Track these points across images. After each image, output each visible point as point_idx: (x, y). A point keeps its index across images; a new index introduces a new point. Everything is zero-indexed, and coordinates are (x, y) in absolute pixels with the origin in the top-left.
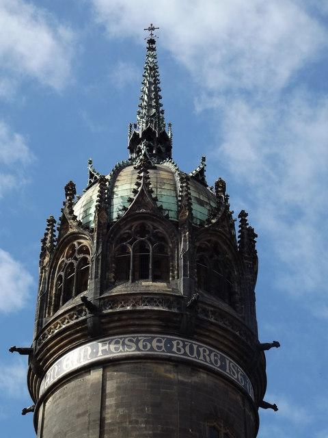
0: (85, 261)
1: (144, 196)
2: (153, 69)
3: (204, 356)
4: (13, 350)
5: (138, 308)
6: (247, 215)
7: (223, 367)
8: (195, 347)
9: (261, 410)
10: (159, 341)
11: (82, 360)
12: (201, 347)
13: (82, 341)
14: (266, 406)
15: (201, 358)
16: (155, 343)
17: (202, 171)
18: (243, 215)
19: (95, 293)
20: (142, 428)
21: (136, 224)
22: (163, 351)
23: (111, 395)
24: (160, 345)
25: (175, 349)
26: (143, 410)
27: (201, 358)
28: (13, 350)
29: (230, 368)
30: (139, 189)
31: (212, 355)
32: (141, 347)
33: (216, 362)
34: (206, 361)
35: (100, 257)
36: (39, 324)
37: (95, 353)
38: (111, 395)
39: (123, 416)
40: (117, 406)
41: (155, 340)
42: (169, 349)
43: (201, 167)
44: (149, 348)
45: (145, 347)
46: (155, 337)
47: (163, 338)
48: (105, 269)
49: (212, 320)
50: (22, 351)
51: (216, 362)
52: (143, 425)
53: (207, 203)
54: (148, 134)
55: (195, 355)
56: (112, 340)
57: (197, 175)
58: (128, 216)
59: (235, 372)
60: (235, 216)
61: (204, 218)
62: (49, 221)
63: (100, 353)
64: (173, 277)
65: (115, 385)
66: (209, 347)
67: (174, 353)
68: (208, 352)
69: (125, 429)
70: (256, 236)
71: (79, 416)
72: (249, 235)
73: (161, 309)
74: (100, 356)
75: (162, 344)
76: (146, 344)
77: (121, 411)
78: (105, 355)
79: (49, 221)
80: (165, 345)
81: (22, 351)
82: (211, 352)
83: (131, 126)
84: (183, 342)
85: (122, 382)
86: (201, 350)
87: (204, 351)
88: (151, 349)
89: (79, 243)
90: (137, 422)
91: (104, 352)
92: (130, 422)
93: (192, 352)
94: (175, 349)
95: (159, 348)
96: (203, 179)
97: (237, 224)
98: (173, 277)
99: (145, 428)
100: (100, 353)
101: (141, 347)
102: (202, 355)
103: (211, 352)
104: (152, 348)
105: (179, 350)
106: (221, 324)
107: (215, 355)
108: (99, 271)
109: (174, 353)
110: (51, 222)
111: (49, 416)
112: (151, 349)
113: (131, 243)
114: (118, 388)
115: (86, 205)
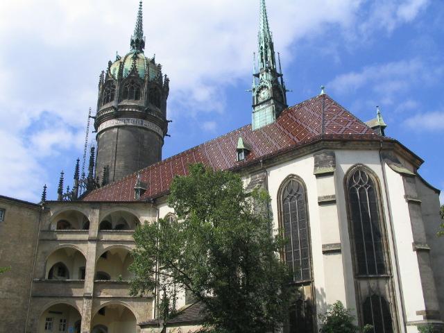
1: (134, 70)
2: (140, 13)
9: (166, 138)
14: (167, 135)
17: (153, 60)
18: (166, 76)
21: (131, 80)
36: (98, 109)
42: (142, 124)
48: (120, 94)
54: (137, 40)
58: (129, 77)
59: (160, 132)
72: (167, 80)
97: (164, 78)
110: (103, 72)
115: (115, 69)
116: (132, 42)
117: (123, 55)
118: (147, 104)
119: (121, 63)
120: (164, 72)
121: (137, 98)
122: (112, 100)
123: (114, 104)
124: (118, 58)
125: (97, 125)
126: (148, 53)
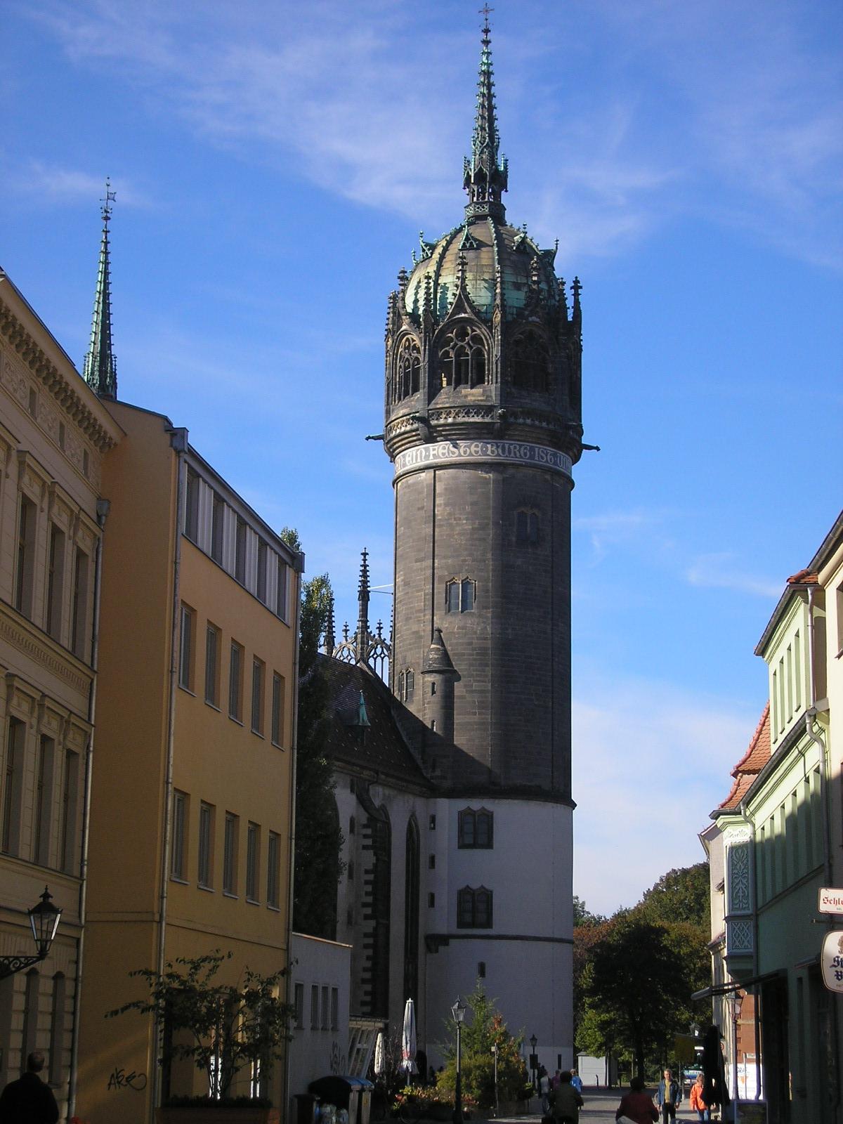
0: (417, 359)
2: (488, 74)
3: (515, 452)
4: (367, 439)
5: (460, 420)
7: (532, 457)
8: (507, 446)
10: (477, 446)
11: (419, 460)
12: (512, 444)
13: (417, 443)
15: (512, 455)
16: (473, 448)
19: (424, 405)
20: (463, 524)
22: (480, 455)
23: (441, 495)
25: (489, 452)
26: (464, 509)
27: (512, 455)
28: (367, 439)
29: (539, 453)
30: (458, 293)
31: (522, 449)
32: (462, 454)
33: (525, 454)
34: (517, 457)
35: (427, 366)
37: (427, 457)
38: (441, 495)
39: (450, 514)
40: (446, 505)
41: (473, 446)
43: (522, 235)
44: (468, 453)
45: (465, 452)
49: (521, 421)
51: (525, 454)
52: (465, 522)
53: (525, 284)
54: (480, 176)
55: (507, 453)
56: (440, 445)
61: (521, 303)
63: (431, 457)
64: (489, 382)
65: (443, 487)
66: (519, 443)
67: (489, 455)
68: (518, 446)
69: (451, 525)
71: (419, 509)
73: (477, 419)
74: (432, 461)
75: (479, 449)
77: (448, 509)
78: (434, 459)
80: (482, 450)
82: (520, 446)
84: (497, 443)
85: (448, 484)
86: (512, 447)
87: (515, 448)
89: (413, 341)
90: (460, 519)
91: (434, 455)
92: (455, 519)
93: (503, 453)
94: (489, 452)
98: (489, 382)
99: (466, 523)
100: (431, 457)
101: (462, 454)
102: (512, 452)
103: (520, 446)
105: (493, 452)
106: (529, 421)
107: (525, 449)
108: (427, 380)
109: (489, 455)
111: (401, 501)
112: (471, 454)
113: (453, 348)
114: (446, 489)
116: (467, 183)
118: (505, 396)
119: (428, 278)
120: (562, 269)
121: (479, 380)
122: (416, 390)
123: (417, 402)
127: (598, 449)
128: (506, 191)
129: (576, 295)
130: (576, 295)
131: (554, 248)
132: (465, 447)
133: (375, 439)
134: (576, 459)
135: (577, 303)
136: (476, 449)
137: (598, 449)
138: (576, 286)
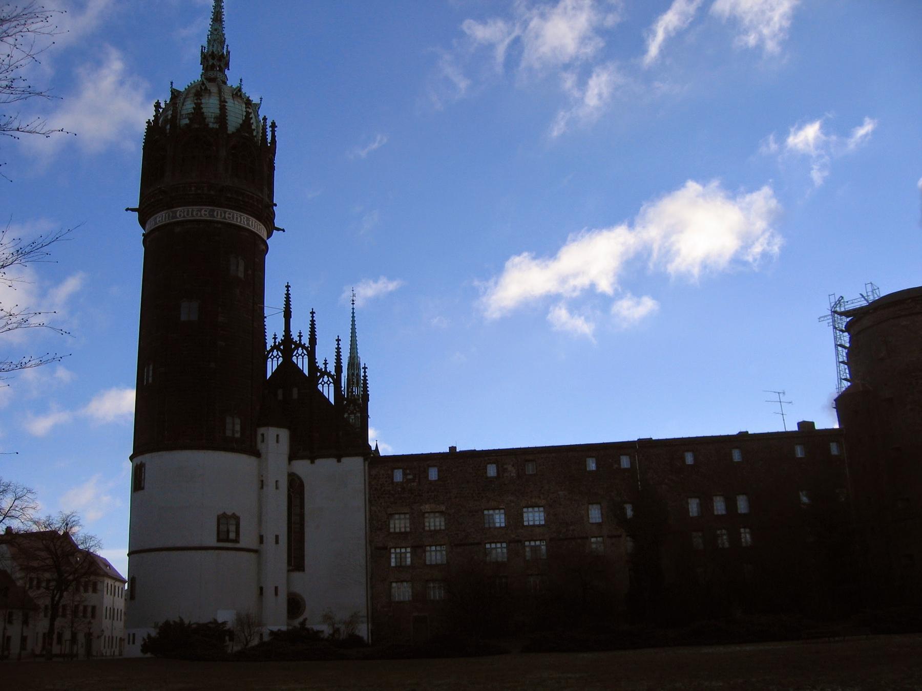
4: (127, 210)
6: (267, 119)
10: (205, 211)
14: (278, 229)
16: (203, 212)
17: (240, 90)
22: (208, 217)
24: (206, 213)
28: (127, 210)
32: (195, 216)
41: (203, 210)
44: (199, 215)
45: (197, 214)
46: (202, 209)
47: (208, 209)
50: (133, 210)
57: (236, 93)
60: (261, 118)
62: (147, 122)
70: (277, 127)
76: (198, 213)
79: (147, 122)
81: (133, 210)
83: (202, 46)
88: (201, 216)
95: (205, 215)
96: (241, 94)
101: (195, 216)
104: (201, 214)
110: (149, 122)
117: (181, 87)
124: (175, 94)
125: (143, 222)
126: (232, 78)
127: (283, 230)
128: (229, 69)
129: (273, 132)
130: (273, 132)
131: (259, 102)
132: (198, 211)
133: (132, 211)
134: (270, 235)
135: (273, 136)
136: (206, 213)
137: (283, 230)
138: (273, 126)
